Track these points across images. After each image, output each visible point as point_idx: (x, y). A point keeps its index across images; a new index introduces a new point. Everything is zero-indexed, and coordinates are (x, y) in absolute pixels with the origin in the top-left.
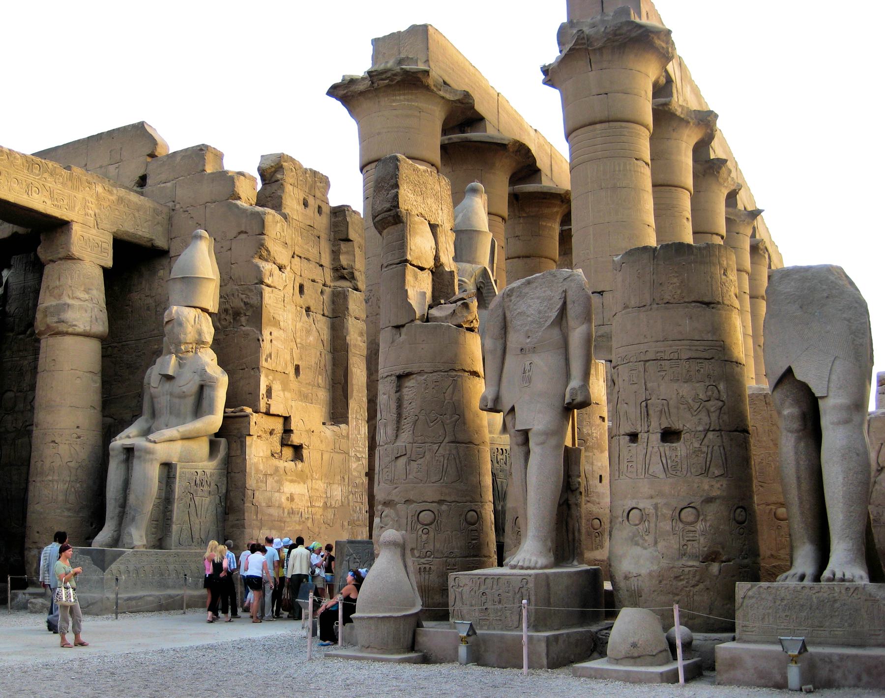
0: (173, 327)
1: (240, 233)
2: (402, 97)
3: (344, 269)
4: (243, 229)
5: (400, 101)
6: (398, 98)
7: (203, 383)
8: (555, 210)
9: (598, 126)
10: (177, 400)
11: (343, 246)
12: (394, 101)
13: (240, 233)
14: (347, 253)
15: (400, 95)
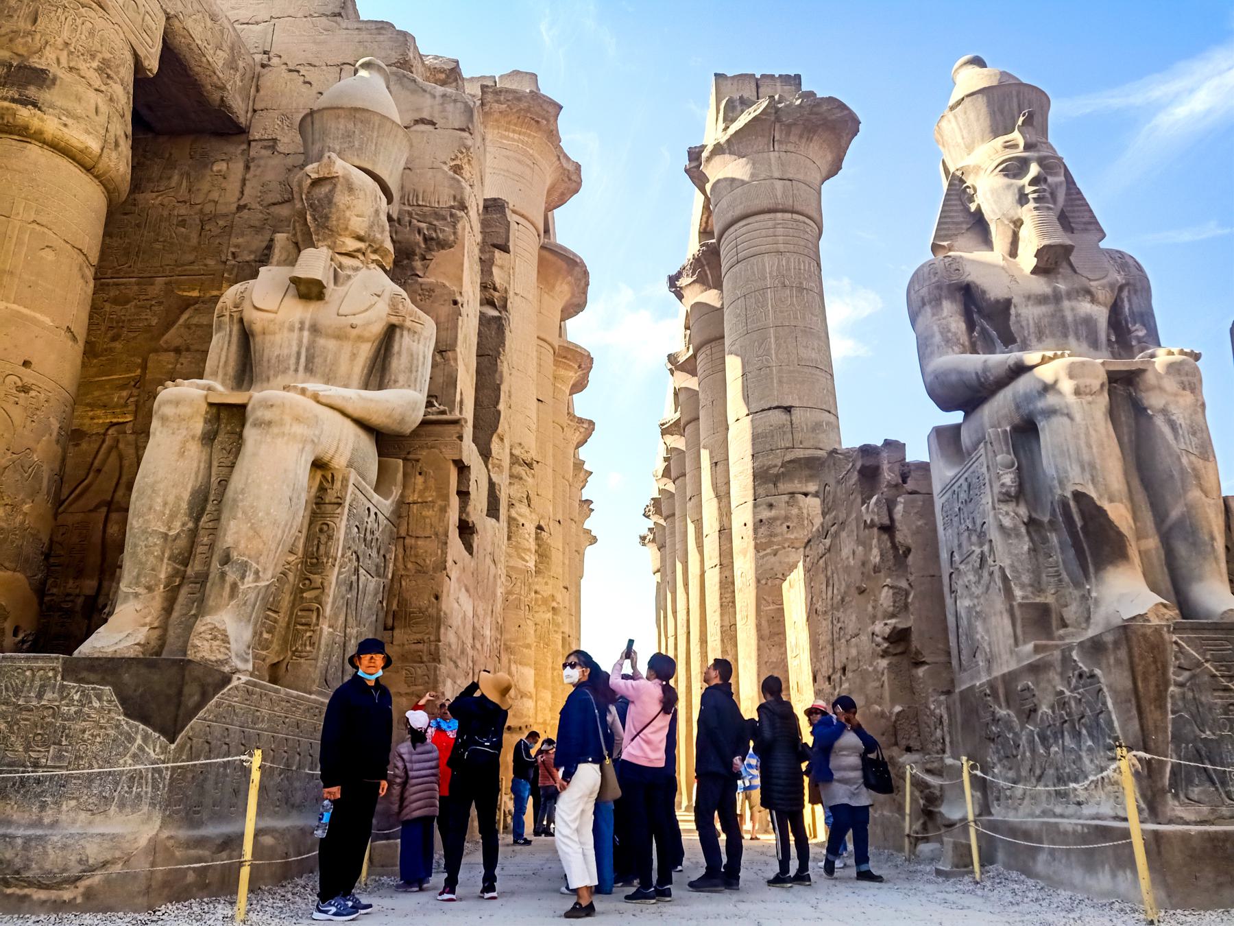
0: (332, 191)
1: (417, 122)
2: (516, 136)
3: (495, 289)
4: (426, 115)
5: (514, 140)
6: (511, 135)
7: (394, 320)
8: (571, 374)
9: (779, 215)
10: (331, 344)
11: (498, 254)
12: (507, 138)
13: (417, 122)
14: (501, 267)
15: (514, 131)
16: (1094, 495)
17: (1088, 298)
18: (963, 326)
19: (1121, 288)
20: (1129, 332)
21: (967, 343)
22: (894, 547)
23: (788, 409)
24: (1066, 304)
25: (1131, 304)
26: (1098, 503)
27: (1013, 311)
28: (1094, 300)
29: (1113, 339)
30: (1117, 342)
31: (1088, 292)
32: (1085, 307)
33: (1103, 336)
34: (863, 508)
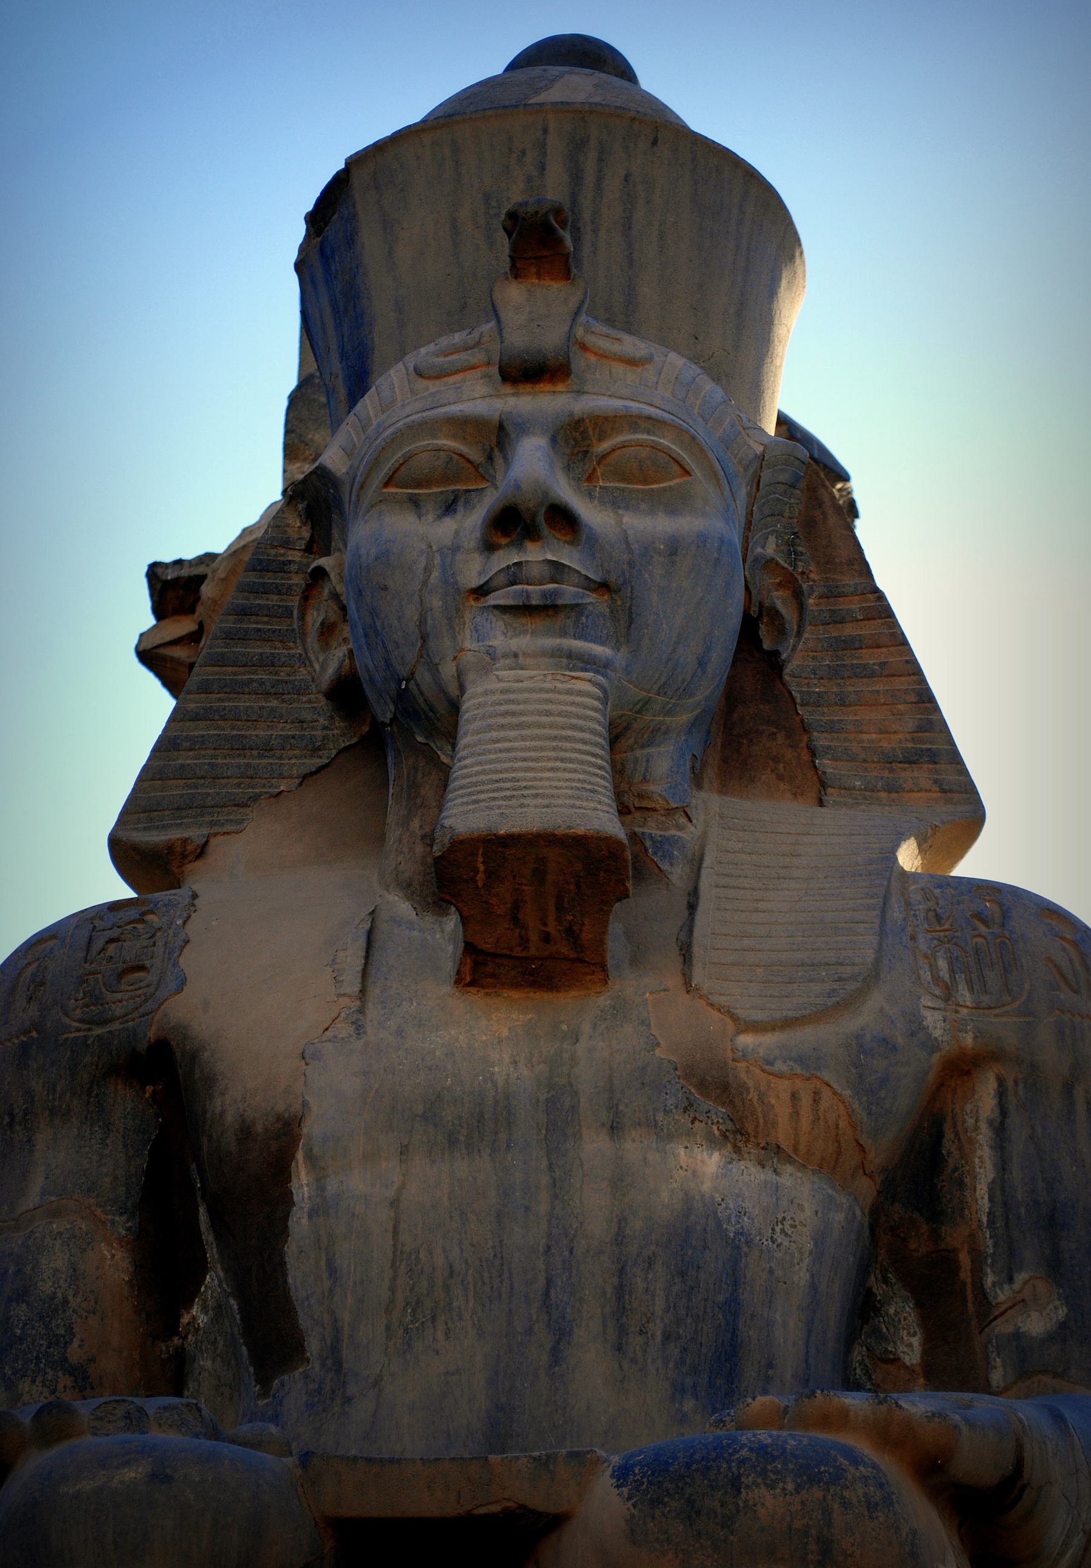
18: (112, 1263)
19: (960, 1068)
20: (986, 1311)
24: (594, 1146)
25: (1003, 1166)
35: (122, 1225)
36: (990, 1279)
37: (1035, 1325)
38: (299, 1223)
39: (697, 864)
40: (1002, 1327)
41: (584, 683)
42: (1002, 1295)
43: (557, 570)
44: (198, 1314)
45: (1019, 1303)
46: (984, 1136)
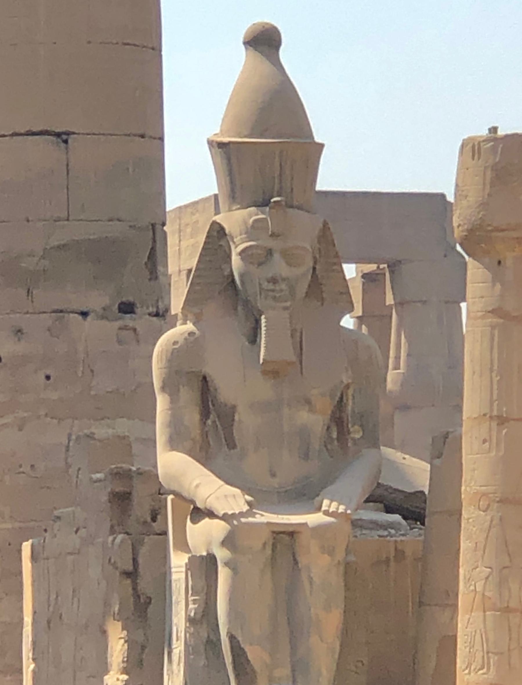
16: (240, 639)
17: (307, 408)
18: (197, 417)
19: (348, 386)
20: (349, 433)
21: (198, 438)
22: (137, 595)
23: (63, 137)
24: (286, 411)
25: (354, 403)
26: (242, 646)
27: (236, 418)
28: (312, 410)
29: (335, 435)
30: (338, 439)
31: (308, 402)
32: (304, 416)
33: (316, 445)
34: (111, 538)
35: (198, 408)
36: (350, 426)
37: (357, 436)
38: (236, 424)
39: (301, 333)
40: (352, 435)
41: (286, 314)
42: (351, 430)
43: (281, 291)
44: (209, 422)
45: (355, 432)
46: (350, 397)
